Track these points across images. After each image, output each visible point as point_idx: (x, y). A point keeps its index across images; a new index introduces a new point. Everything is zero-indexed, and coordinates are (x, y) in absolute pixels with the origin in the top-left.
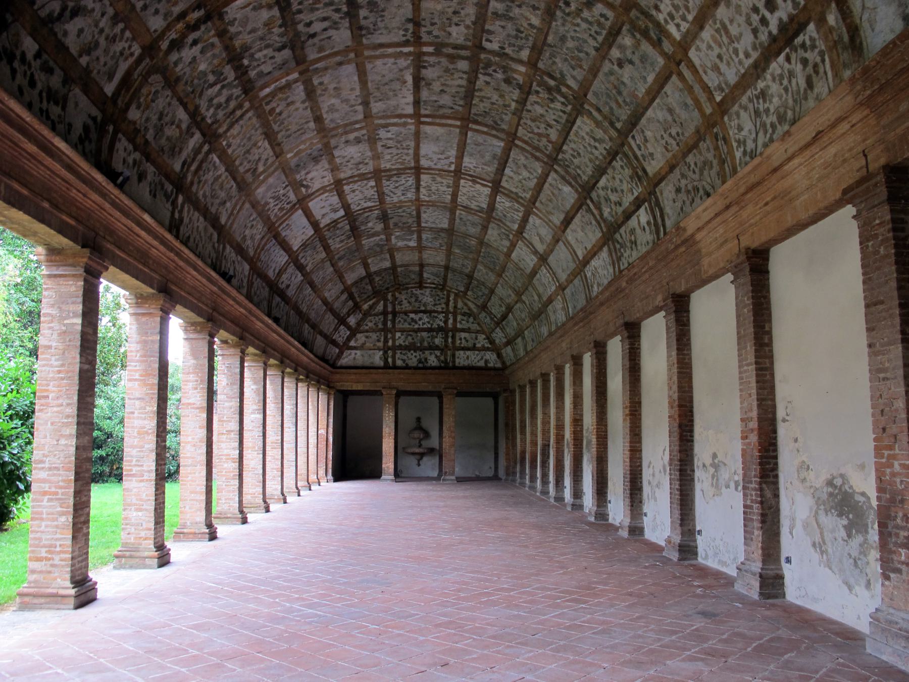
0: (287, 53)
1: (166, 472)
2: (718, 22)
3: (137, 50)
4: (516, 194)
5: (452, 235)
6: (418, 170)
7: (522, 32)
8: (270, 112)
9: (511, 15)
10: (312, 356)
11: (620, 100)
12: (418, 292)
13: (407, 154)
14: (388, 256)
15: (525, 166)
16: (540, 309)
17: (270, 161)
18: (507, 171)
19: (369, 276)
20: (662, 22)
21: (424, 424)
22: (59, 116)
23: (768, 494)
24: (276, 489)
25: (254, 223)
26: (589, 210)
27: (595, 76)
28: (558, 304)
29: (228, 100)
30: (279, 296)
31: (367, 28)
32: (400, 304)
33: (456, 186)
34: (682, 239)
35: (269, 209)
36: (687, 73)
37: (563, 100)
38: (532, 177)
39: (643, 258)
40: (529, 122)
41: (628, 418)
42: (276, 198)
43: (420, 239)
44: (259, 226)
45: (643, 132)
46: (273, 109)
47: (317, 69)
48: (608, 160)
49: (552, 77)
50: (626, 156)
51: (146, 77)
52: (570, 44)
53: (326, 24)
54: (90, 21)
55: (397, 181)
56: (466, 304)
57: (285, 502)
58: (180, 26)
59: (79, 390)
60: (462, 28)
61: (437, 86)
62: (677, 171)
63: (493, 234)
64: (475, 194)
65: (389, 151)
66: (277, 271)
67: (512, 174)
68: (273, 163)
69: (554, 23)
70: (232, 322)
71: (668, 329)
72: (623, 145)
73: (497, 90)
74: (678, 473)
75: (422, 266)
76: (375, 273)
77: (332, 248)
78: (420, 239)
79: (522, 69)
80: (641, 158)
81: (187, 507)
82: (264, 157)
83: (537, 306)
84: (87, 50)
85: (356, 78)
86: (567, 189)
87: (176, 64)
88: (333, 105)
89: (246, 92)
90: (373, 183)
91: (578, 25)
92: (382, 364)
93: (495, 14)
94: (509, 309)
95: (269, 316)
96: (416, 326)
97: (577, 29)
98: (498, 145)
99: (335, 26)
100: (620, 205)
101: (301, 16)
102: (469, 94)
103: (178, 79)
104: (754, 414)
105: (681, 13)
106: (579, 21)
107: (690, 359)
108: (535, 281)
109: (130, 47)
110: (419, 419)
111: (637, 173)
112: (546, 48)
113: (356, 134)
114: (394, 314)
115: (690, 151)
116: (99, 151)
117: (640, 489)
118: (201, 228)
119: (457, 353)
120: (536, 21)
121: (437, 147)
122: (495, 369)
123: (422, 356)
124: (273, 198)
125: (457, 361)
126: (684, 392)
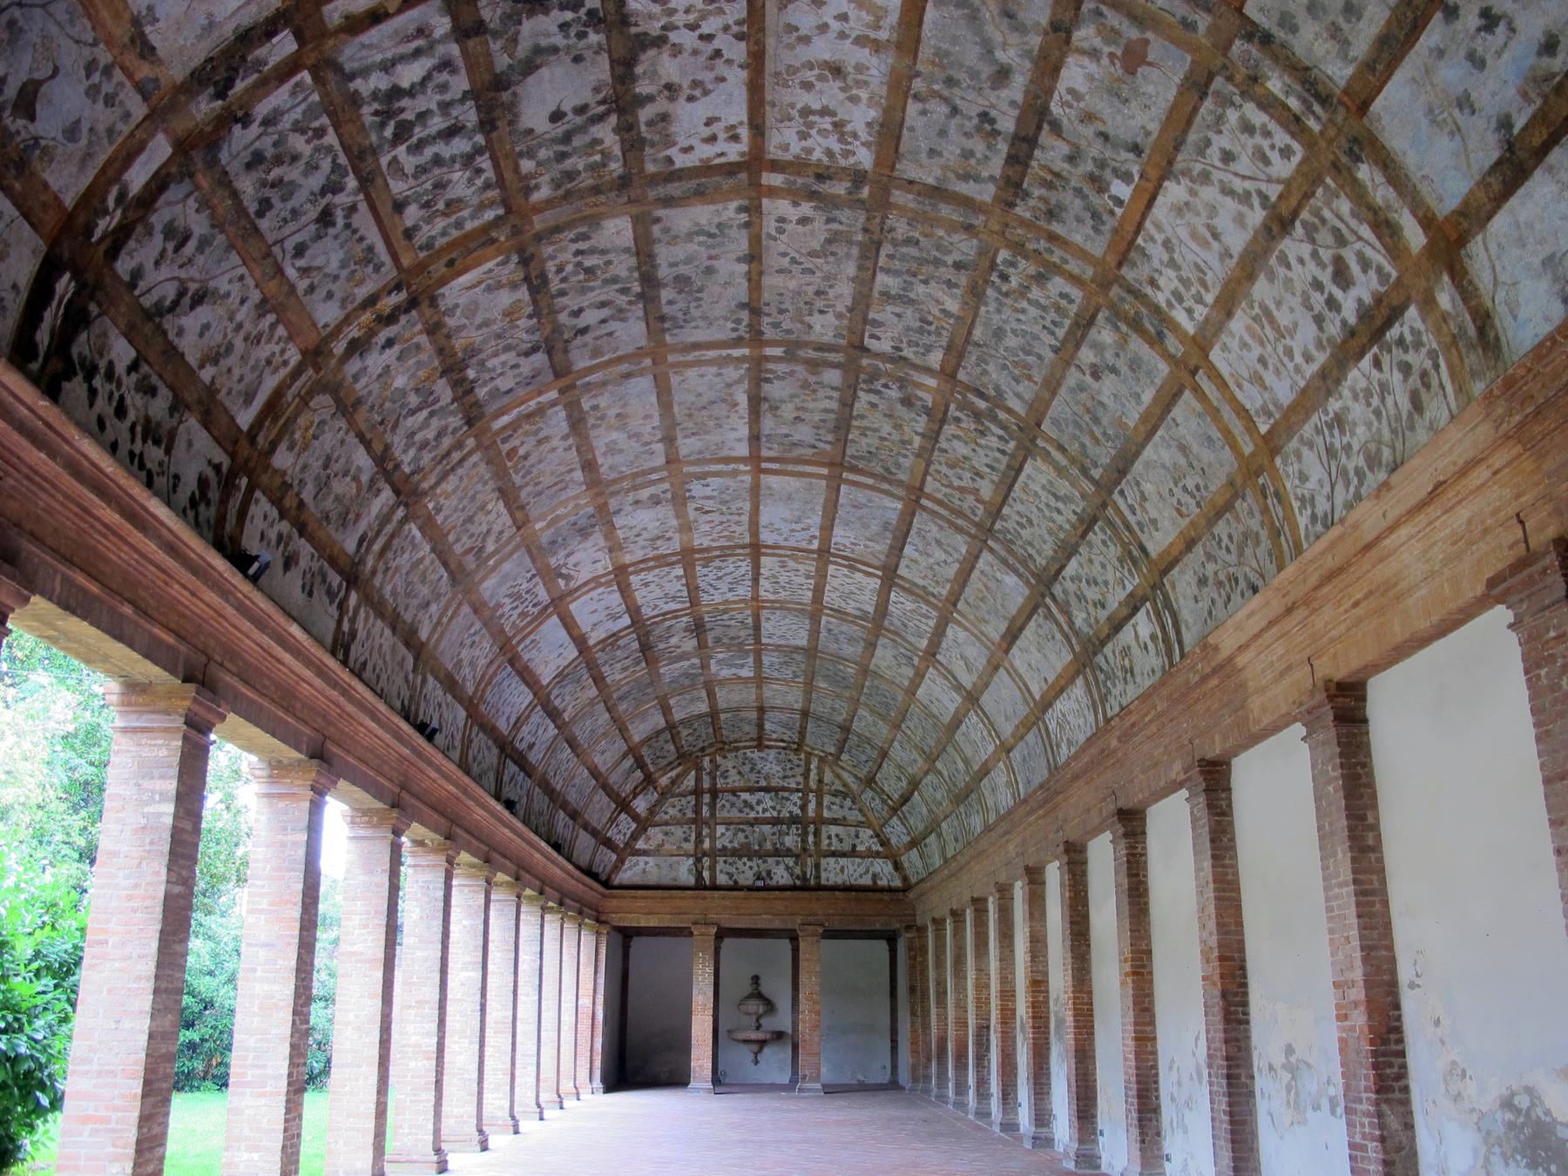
0: (540, 358)
1: (306, 1073)
2: (1256, 305)
3: (294, 356)
4: (924, 588)
5: (815, 657)
6: (756, 550)
7: (930, 324)
8: (508, 454)
9: (912, 296)
10: (570, 867)
11: (1097, 431)
12: (756, 755)
13: (738, 523)
14: (704, 694)
15: (938, 542)
16: (967, 784)
17: (506, 536)
18: (908, 550)
19: (671, 727)
20: (1164, 305)
21: (765, 988)
22: (161, 464)
23: (1394, 1123)
24: (501, 1108)
25: (477, 638)
26: (1049, 615)
27: (1054, 393)
28: (999, 776)
29: (439, 436)
30: (516, 763)
31: (673, 318)
32: (724, 775)
33: (822, 576)
34: (1213, 664)
35: (502, 616)
36: (1208, 387)
37: (1001, 432)
38: (950, 560)
39: (1144, 697)
40: (944, 469)
41: (1129, 980)
42: (516, 597)
43: (758, 663)
44: (485, 644)
45: (1138, 484)
46: (514, 450)
47: (589, 383)
48: (1079, 532)
49: (981, 395)
50: (1111, 524)
51: (304, 400)
52: (1011, 341)
53: (605, 312)
54: (221, 311)
55: (720, 568)
56: (838, 777)
57: (516, 1132)
58: (367, 317)
59: (161, 932)
60: (830, 317)
61: (788, 411)
62: (1199, 550)
63: (884, 657)
64: (854, 590)
66: (512, 721)
67: (916, 555)
68: (512, 538)
69: (983, 309)
70: (433, 808)
71: (1194, 820)
72: (1104, 505)
73: (890, 416)
74: (1224, 1082)
75: (761, 710)
76: (682, 722)
77: (608, 680)
78: (758, 663)
79: (932, 382)
80: (1136, 528)
81: (341, 1142)
82: (497, 528)
83: (962, 779)
84: (213, 358)
85: (654, 399)
86: (1011, 580)
87: (356, 378)
88: (614, 442)
89: (469, 422)
90: (679, 571)
91: (1023, 311)
92: (692, 881)
93: (886, 295)
94: (914, 784)
95: (497, 797)
96: (753, 815)
97: (1021, 317)
98: (893, 507)
100: (1103, 607)
101: (564, 300)
102: (843, 424)
103: (359, 402)
104: (1358, 974)
105: (1193, 291)
106: (1024, 304)
107: (1236, 874)
108: (958, 736)
109: (283, 351)
110: (756, 979)
111: (1130, 552)
112: (970, 348)
114: (714, 793)
115: (1219, 515)
116: (221, 519)
117: (1156, 1110)
118: (386, 648)
119: (824, 861)
120: (953, 306)
121: (789, 511)
122: (890, 890)
123: (763, 867)
124: (510, 596)
125: (824, 875)
126: (1227, 933)
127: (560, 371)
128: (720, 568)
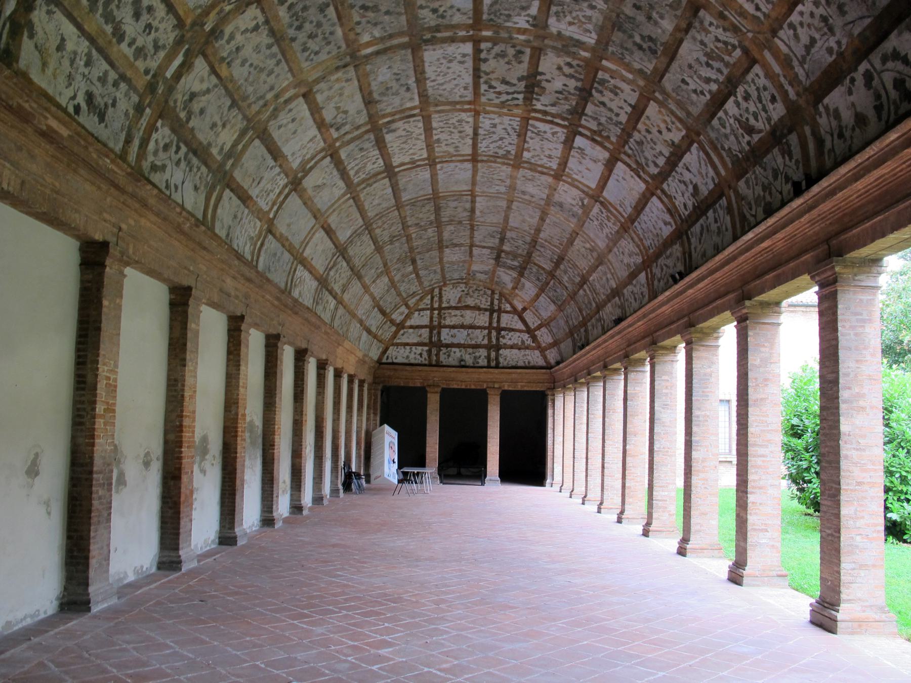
6: (474, 158)
33: (430, 147)
55: (499, 148)
66: (668, 218)
99: (512, 238)
127: (534, 243)
128: (499, 148)
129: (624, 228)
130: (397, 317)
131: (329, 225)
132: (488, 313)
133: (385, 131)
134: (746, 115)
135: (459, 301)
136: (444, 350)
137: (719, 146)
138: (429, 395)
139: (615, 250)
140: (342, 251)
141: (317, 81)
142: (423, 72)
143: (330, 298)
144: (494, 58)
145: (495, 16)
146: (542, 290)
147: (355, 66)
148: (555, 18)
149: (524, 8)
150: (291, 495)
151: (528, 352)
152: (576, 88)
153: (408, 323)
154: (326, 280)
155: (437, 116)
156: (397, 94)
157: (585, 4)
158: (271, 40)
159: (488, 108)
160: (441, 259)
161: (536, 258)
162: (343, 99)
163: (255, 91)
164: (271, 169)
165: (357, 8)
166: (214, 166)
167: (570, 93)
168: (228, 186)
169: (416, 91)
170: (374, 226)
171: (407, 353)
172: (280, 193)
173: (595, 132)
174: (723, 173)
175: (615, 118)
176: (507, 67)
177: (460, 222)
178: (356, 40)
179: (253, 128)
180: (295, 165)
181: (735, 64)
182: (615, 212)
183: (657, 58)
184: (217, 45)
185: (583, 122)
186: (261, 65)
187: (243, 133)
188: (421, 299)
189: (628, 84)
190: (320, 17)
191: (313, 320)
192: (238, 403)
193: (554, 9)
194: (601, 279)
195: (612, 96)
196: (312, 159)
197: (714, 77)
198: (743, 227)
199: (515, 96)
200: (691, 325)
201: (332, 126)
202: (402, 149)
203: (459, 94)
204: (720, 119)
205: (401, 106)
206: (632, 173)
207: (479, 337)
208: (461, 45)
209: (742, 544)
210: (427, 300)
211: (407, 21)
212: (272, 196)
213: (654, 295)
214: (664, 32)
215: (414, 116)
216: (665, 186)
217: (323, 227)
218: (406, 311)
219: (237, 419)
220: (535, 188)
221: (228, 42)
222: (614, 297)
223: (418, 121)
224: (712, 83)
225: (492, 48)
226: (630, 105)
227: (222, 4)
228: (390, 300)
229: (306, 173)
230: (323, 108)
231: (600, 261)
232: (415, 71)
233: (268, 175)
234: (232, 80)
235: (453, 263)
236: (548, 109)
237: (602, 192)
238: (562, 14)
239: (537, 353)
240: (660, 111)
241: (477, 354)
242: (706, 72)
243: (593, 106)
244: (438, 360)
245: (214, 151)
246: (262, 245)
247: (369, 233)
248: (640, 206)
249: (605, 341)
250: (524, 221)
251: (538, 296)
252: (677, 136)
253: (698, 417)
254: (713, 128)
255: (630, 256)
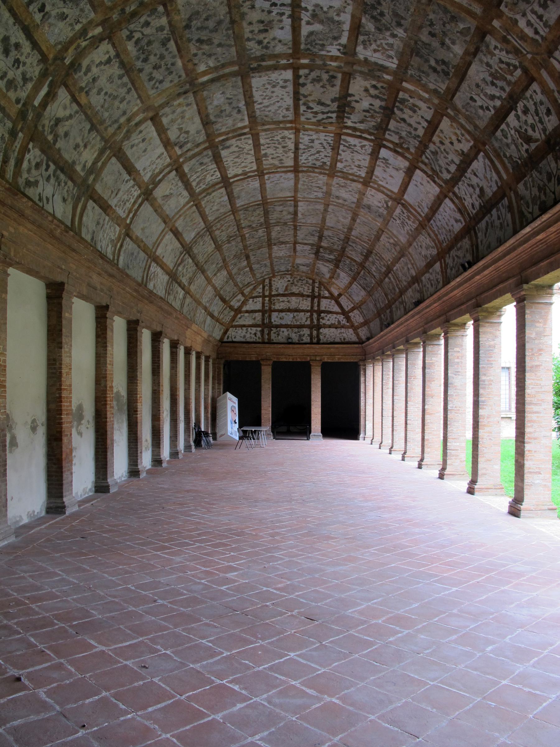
0: (350, 243)
4: (210, 194)
6: (296, 169)
13: (304, 182)
18: (226, 198)
35: (411, 230)
55: (317, 160)
65: (317, 185)
66: (458, 216)
82: (387, 240)
90: (339, 165)
99: (329, 236)
113: (337, 201)
124: (403, 227)
127: (347, 239)
129: (422, 225)
130: (235, 304)
131: (177, 229)
132: (310, 299)
133: (220, 148)
134: (525, 127)
135: (286, 289)
136: (274, 330)
137: (502, 154)
138: (263, 367)
139: (415, 244)
140: (187, 249)
141: (162, 106)
142: (251, 96)
143: (179, 289)
144: (311, 82)
145: (311, 46)
146: (354, 279)
147: (194, 93)
148: (362, 47)
149: (335, 38)
150: (153, 451)
151: (343, 330)
152: (381, 107)
153: (244, 309)
154: (175, 274)
155: (264, 134)
156: (230, 115)
157: (388, 33)
158: (122, 72)
159: (306, 126)
160: (270, 255)
161: (350, 252)
162: (185, 121)
163: (110, 117)
164: (127, 182)
165: (194, 42)
166: (79, 181)
167: (375, 112)
168: (91, 198)
169: (246, 113)
170: (214, 228)
171: (244, 333)
172: (135, 202)
173: (397, 144)
174: (505, 177)
175: (413, 132)
176: (322, 90)
177: (285, 224)
178: (194, 70)
179: (110, 148)
180: (146, 178)
181: (516, 82)
182: (414, 212)
183: (449, 79)
184: (76, 77)
185: (387, 136)
186: (115, 94)
187: (102, 152)
188: (255, 288)
189: (425, 102)
190: (163, 50)
191: (166, 307)
192: (106, 377)
193: (361, 38)
194: (403, 268)
195: (411, 113)
196: (160, 172)
197: (498, 94)
198: (521, 223)
199: (330, 115)
200: (478, 305)
201: (176, 145)
202: (235, 163)
203: (282, 114)
204: (502, 131)
205: (234, 126)
206: (428, 179)
207: (303, 318)
208: (283, 72)
209: (520, 484)
210: (260, 289)
211: (237, 52)
212: (128, 205)
213: (447, 281)
214: (455, 55)
215: (245, 134)
216: (456, 189)
217: (171, 230)
218: (243, 299)
219: (106, 391)
220: (347, 193)
221: (85, 74)
222: (414, 283)
223: (248, 138)
224: (496, 100)
225: (309, 74)
226: (426, 121)
227: (79, 41)
228: (229, 289)
229: (156, 185)
230: (168, 129)
231: (402, 254)
232: (245, 95)
233: (124, 188)
234: (90, 106)
235: (280, 258)
236: (358, 126)
237: (403, 196)
238: (368, 43)
239: (351, 330)
240: (452, 125)
241: (302, 333)
242: (491, 90)
243: (395, 122)
244: (269, 339)
245: (78, 168)
246: (121, 246)
247: (210, 234)
248: (435, 207)
249: (407, 320)
250: (338, 221)
251: (351, 284)
252: (466, 146)
253: (484, 381)
254: (497, 139)
255: (427, 249)
